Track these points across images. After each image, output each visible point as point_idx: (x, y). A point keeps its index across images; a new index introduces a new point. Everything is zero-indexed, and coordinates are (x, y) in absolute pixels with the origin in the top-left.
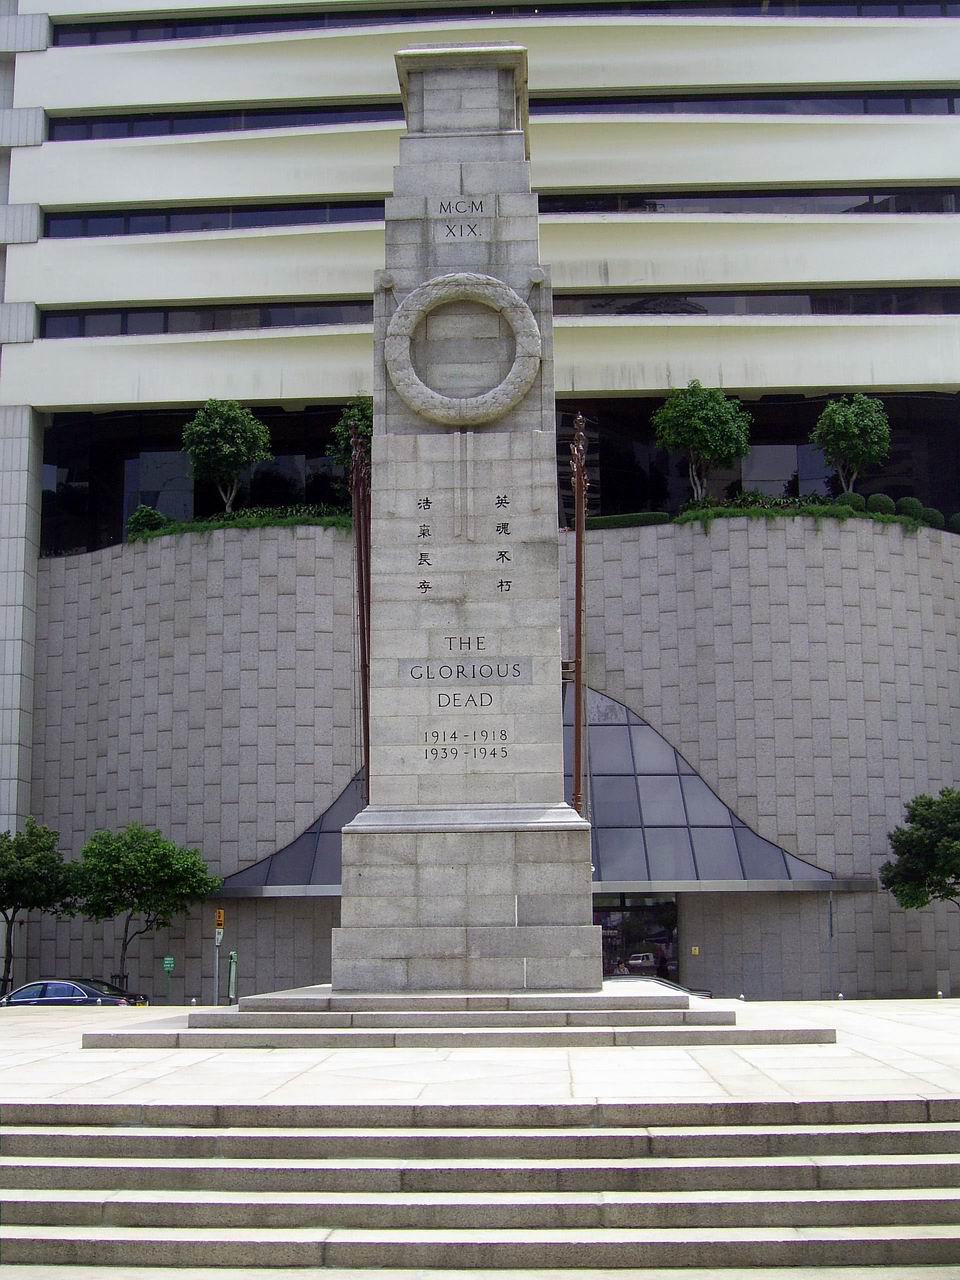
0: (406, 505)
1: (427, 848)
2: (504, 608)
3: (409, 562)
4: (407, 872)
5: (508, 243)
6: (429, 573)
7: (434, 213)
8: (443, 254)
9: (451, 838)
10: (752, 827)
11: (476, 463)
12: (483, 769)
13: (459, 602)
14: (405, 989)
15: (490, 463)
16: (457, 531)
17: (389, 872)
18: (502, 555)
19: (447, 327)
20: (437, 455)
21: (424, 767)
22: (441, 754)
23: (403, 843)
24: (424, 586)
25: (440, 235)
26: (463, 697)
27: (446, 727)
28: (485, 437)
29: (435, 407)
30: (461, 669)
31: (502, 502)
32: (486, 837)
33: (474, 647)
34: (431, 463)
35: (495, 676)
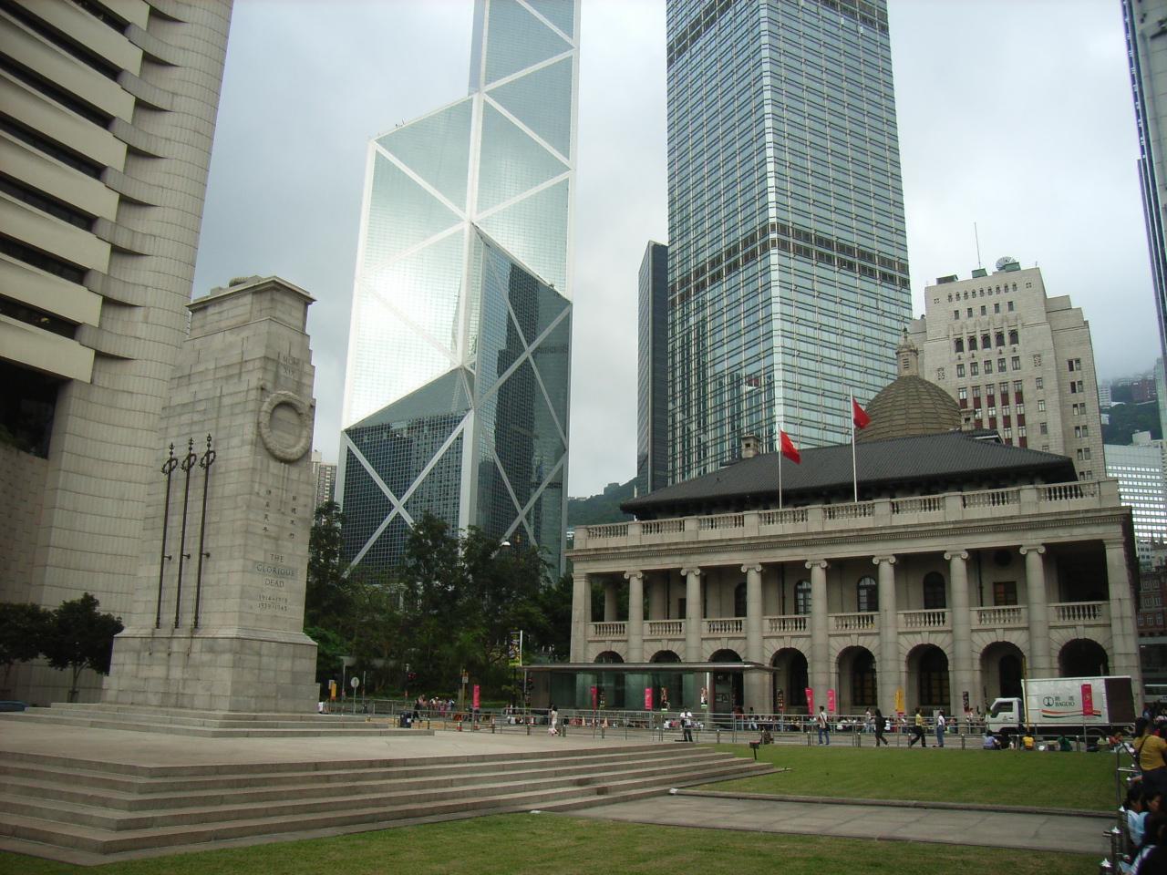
0: (263, 492)
2: (290, 545)
3: (261, 518)
4: (256, 658)
5: (304, 384)
11: (288, 479)
12: (278, 614)
13: (277, 539)
14: (255, 711)
19: (284, 414)
20: (275, 472)
21: (257, 611)
23: (256, 644)
25: (282, 372)
31: (294, 498)
34: (273, 475)
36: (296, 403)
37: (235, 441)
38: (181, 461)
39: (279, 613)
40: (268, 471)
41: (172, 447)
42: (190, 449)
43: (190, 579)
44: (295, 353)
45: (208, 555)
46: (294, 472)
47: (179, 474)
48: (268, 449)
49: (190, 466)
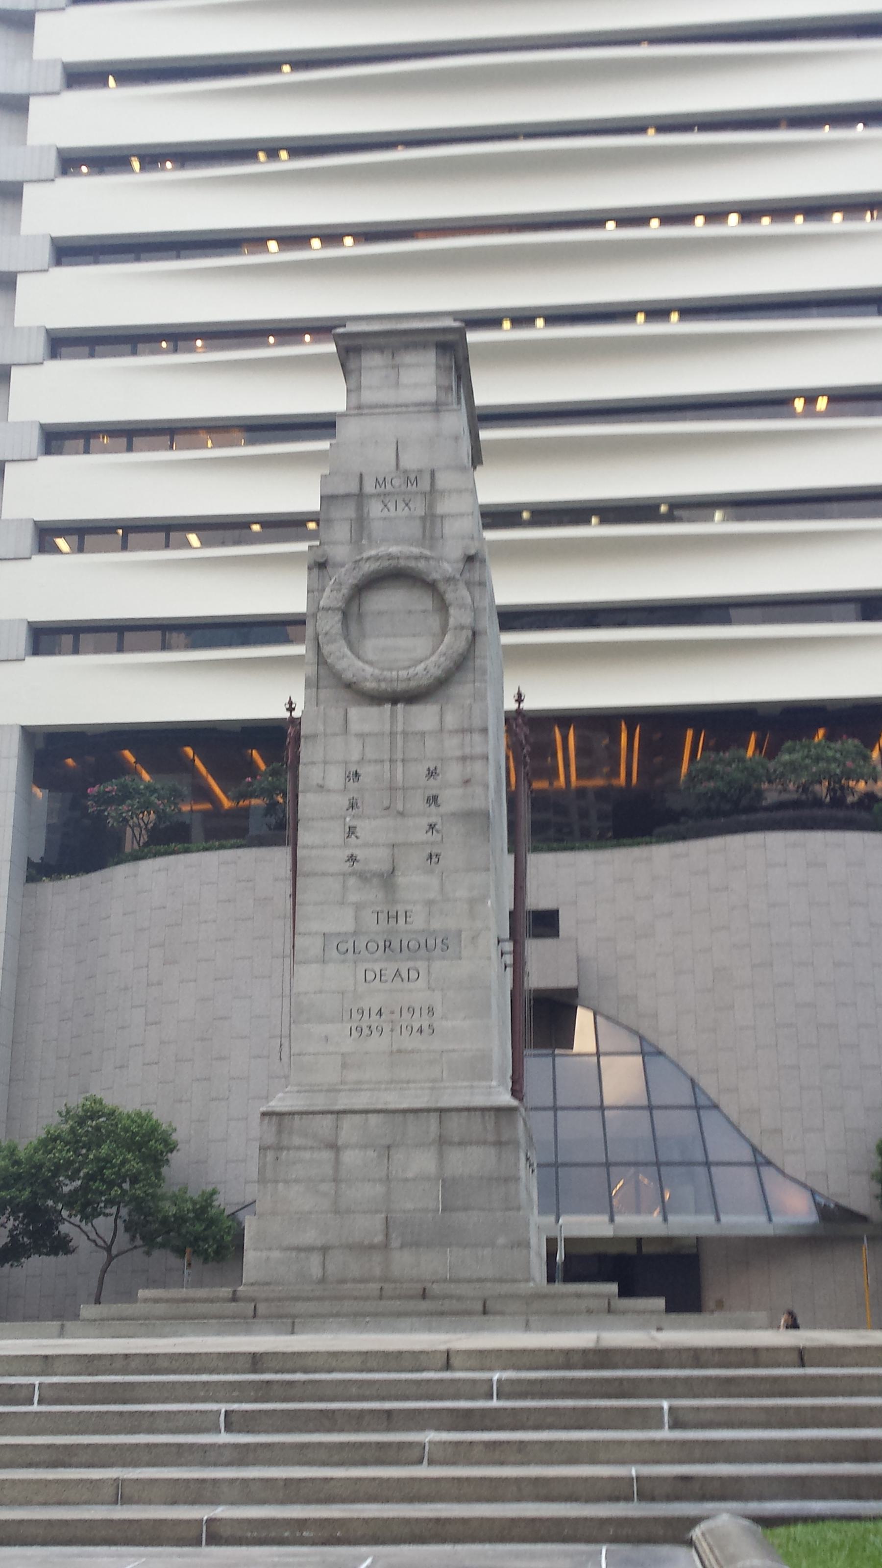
0: (335, 777)
1: (349, 1129)
2: (434, 882)
3: (336, 835)
4: (327, 1155)
5: (442, 517)
6: (357, 846)
8: (377, 528)
9: (373, 1119)
10: (779, 1163)
11: (405, 734)
15: (423, 734)
16: (386, 803)
17: (307, 1155)
18: (432, 827)
20: (366, 728)
21: (348, 1045)
22: (366, 1031)
24: (352, 859)
25: (375, 509)
26: (390, 972)
27: (373, 1002)
28: (416, 709)
29: (366, 679)
30: (387, 944)
31: (432, 773)
32: (410, 1117)
33: (401, 920)
34: (362, 736)
35: (423, 950)
36: (412, 564)
39: (410, 1042)
48: (349, 686)
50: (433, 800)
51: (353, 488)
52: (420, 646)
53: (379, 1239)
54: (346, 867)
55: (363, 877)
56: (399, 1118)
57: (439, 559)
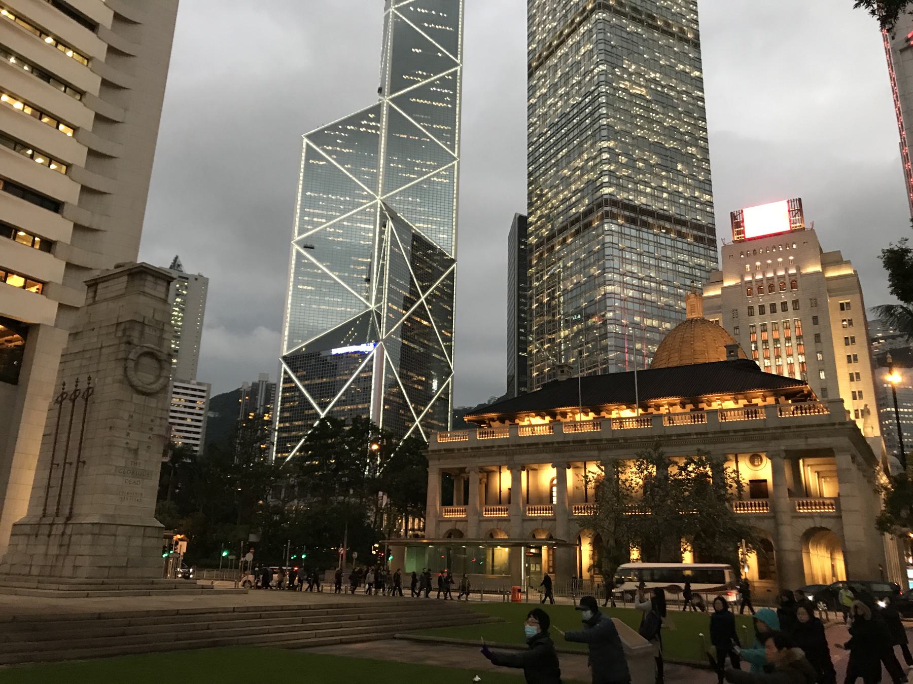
0: (126, 416)
5: (164, 339)
7: (146, 322)
18: (150, 438)
19: (146, 360)
24: (127, 443)
25: (147, 330)
31: (152, 421)
36: (157, 353)
37: (109, 380)
38: (82, 392)
40: (131, 401)
41: (64, 384)
42: (76, 386)
43: (69, 481)
44: (158, 317)
45: (84, 462)
46: (153, 402)
47: (67, 404)
49: (76, 397)
50: (151, 429)
51: (141, 320)
52: (151, 378)
53: (125, 565)
54: (125, 446)
55: (130, 450)
56: (133, 528)
57: (162, 352)
